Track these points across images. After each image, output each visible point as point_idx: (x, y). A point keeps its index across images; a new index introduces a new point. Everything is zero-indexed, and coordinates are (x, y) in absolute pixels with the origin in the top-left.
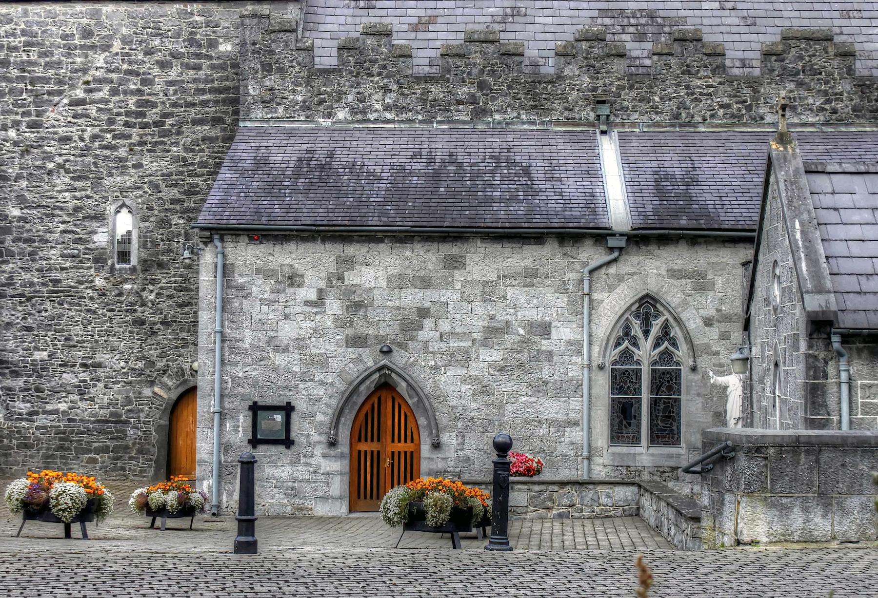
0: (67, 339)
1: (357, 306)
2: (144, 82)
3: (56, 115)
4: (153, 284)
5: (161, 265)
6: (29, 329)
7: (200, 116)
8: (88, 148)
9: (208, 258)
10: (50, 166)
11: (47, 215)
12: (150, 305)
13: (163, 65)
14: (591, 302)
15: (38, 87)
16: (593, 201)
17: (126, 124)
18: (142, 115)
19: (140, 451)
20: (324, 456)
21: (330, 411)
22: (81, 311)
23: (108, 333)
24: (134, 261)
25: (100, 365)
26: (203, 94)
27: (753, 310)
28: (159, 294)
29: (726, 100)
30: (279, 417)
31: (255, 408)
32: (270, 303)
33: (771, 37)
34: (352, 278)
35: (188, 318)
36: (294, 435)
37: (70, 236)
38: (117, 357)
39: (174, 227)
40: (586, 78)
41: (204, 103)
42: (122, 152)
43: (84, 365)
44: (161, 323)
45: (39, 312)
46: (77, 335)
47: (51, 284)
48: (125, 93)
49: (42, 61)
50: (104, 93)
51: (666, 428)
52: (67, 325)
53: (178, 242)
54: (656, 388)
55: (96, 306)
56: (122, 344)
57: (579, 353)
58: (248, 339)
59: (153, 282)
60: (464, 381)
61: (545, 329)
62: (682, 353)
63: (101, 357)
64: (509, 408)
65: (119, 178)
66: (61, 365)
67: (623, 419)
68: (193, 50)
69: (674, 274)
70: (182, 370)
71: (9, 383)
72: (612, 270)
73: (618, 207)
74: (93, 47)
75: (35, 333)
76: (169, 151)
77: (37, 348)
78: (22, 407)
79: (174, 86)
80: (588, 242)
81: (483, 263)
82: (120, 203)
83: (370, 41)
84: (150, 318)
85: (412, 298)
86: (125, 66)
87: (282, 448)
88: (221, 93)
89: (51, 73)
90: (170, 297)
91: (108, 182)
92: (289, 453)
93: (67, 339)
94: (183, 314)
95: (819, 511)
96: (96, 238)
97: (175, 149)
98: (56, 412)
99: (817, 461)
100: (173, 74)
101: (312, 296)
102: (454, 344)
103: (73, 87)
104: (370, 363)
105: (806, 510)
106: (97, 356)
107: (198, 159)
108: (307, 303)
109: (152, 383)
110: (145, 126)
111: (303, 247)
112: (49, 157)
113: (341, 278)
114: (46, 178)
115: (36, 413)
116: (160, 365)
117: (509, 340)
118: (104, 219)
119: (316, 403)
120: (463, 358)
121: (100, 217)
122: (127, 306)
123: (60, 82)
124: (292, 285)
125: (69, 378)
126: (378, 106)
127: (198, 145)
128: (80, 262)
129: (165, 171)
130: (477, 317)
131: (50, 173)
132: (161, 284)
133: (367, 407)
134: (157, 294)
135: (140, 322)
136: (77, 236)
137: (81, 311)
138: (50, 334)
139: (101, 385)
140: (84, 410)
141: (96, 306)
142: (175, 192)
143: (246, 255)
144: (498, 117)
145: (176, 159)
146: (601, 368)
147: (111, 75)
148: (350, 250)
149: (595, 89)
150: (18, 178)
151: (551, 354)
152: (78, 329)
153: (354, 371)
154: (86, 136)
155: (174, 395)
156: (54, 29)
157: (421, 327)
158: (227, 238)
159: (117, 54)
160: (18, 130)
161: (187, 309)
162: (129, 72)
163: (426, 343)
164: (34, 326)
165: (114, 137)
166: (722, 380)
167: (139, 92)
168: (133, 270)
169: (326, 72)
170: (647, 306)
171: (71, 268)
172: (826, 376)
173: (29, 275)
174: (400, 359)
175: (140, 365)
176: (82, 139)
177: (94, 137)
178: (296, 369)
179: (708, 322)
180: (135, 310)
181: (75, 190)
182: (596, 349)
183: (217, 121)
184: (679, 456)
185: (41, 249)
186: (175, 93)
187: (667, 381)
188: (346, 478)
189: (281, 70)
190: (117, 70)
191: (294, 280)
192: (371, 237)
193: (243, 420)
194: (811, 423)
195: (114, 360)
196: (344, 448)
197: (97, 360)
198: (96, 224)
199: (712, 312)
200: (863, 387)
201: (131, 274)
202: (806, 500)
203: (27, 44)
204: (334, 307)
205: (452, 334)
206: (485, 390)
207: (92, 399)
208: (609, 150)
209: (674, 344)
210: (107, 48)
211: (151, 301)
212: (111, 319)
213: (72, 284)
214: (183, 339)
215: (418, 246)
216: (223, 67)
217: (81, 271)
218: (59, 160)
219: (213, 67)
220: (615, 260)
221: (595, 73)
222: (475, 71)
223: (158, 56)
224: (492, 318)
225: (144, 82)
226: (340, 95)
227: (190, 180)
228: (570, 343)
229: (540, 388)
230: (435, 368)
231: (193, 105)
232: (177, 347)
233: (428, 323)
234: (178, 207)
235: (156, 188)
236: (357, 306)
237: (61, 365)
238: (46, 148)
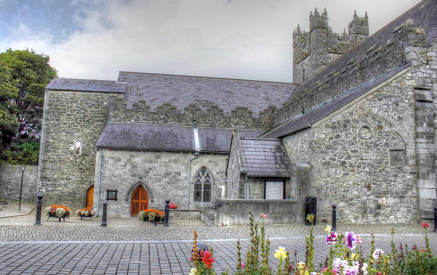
1: (134, 167)
2: (85, 111)
3: (63, 118)
5: (87, 155)
6: (53, 170)
8: (70, 126)
9: (98, 154)
10: (61, 130)
13: (90, 107)
14: (190, 168)
15: (59, 111)
16: (192, 143)
17: (80, 121)
18: (84, 119)
19: (79, 201)
20: (125, 203)
21: (127, 192)
23: (73, 171)
24: (80, 154)
25: (70, 179)
27: (228, 171)
29: (223, 122)
30: (114, 193)
31: (108, 191)
32: (113, 165)
33: (234, 108)
34: (133, 160)
36: (117, 198)
40: (191, 115)
41: (99, 117)
42: (79, 127)
43: (66, 179)
48: (80, 113)
49: (61, 104)
50: (75, 113)
51: (207, 198)
54: (205, 188)
57: (187, 180)
58: (107, 174)
59: (84, 159)
60: (159, 186)
61: (179, 174)
62: (211, 180)
63: (70, 177)
64: (170, 192)
67: (197, 195)
68: (98, 104)
69: (210, 162)
71: (47, 183)
72: (196, 160)
73: (197, 146)
74: (73, 102)
77: (55, 174)
78: (50, 189)
80: (190, 153)
81: (165, 158)
83: (140, 104)
85: (148, 165)
86: (81, 107)
87: (114, 201)
89: (62, 108)
90: (89, 163)
91: (75, 134)
92: (116, 202)
95: (241, 218)
96: (71, 148)
98: (59, 190)
99: (241, 206)
100: (92, 109)
101: (124, 164)
102: (157, 177)
103: (68, 111)
104: (137, 181)
105: (238, 218)
108: (122, 166)
109: (83, 184)
110: (85, 121)
111: (122, 152)
112: (61, 128)
113: (131, 160)
115: (54, 190)
116: (85, 179)
117: (171, 176)
119: (123, 191)
120: (159, 180)
121: (72, 143)
123: (65, 110)
124: (118, 161)
125: (62, 182)
126: (142, 119)
130: (163, 170)
131: (61, 132)
133: (136, 191)
135: (81, 169)
139: (70, 184)
140: (66, 190)
143: (107, 154)
144: (170, 123)
145: (92, 130)
146: (192, 183)
148: (133, 153)
149: (193, 118)
150: (53, 132)
151: (180, 180)
153: (133, 182)
155: (88, 187)
156: (64, 97)
157: (149, 172)
158: (103, 149)
162: (81, 108)
163: (150, 176)
166: (220, 187)
167: (84, 113)
168: (80, 156)
169: (129, 110)
170: (203, 169)
172: (244, 187)
174: (144, 180)
175: (80, 179)
176: (69, 124)
177: (72, 123)
178: (119, 182)
179: (218, 173)
181: (66, 136)
182: (191, 179)
183: (102, 121)
184: (210, 205)
187: (208, 187)
188: (130, 209)
189: (118, 110)
190: (79, 108)
191: (119, 160)
192: (138, 150)
193: (105, 193)
194: (240, 197)
196: (130, 201)
199: (219, 171)
200: (252, 189)
202: (239, 215)
203: (57, 101)
204: (128, 167)
205: (157, 174)
206: (164, 188)
207: (68, 187)
208: (196, 132)
209: (210, 178)
210: (77, 102)
215: (149, 153)
216: (105, 108)
218: (63, 129)
219: (102, 108)
220: (196, 158)
221: (193, 114)
222: (165, 112)
223: (89, 105)
224: (167, 171)
225: (85, 111)
226: (133, 116)
227: (95, 135)
228: (185, 177)
229: (178, 188)
230: (153, 182)
231: (97, 117)
233: (151, 171)
235: (87, 136)
236: (134, 167)
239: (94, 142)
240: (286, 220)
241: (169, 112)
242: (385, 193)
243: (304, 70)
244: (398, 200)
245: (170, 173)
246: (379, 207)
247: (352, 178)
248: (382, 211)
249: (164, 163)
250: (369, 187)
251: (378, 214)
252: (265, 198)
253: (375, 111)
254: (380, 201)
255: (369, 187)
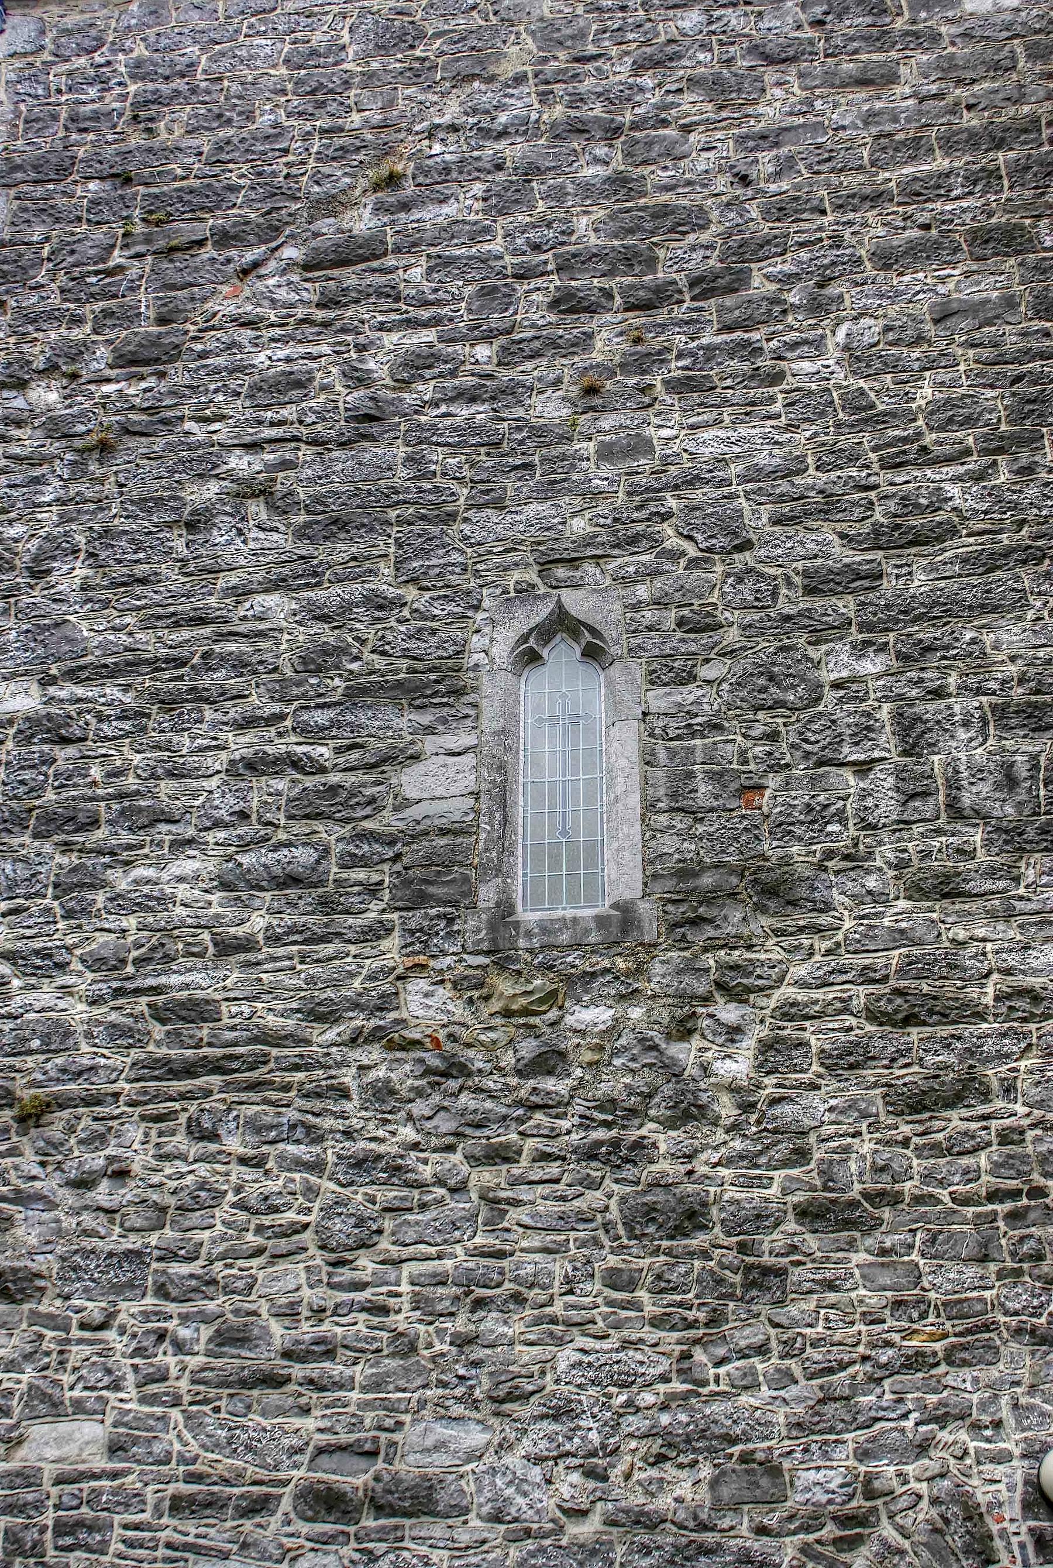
0: (231, 1338)
4: (737, 995)
5: (775, 891)
7: (914, 233)
11: (168, 703)
12: (726, 1108)
22: (316, 1167)
26: (913, 158)
28: (774, 1052)
35: (971, 1175)
37: (280, 785)
38: (538, 1437)
39: (830, 696)
43: (324, 1502)
44: (803, 1213)
45: (83, 1183)
46: (290, 1313)
47: (158, 1031)
52: (229, 1256)
53: (863, 768)
55: (408, 1133)
56: (566, 1356)
65: (533, 509)
66: (178, 1505)
70: (972, 1514)
75: (48, 1306)
76: (776, 378)
77: (48, 1405)
79: (777, 145)
82: (543, 611)
84: (727, 1188)
88: (999, 145)
90: (846, 1061)
93: (231, 1338)
94: (936, 1150)
96: (411, 781)
97: (807, 366)
106: (411, 1435)
107: (926, 393)
114: (179, 546)
118: (458, 692)
121: (439, 687)
122: (586, 1123)
127: (919, 340)
128: (326, 905)
129: (762, 459)
131: (196, 523)
132: (788, 991)
134: (766, 1047)
136: (309, 782)
137: (316, 1167)
138: (128, 1309)
141: (408, 1133)
142: (826, 543)
145: (810, 405)
147: (490, 149)
152: (292, 1279)
154: (377, 366)
159: (519, 79)
160: (74, 376)
161: (955, 1120)
164: (40, 1263)
165: (506, 358)
171: (274, 939)
173: (45, 996)
175: (685, 1488)
180: (638, 1145)
181: (314, 577)
185: (119, 857)
186: (785, 167)
195: (513, 1460)
197: (408, 1467)
198: (406, 721)
201: (610, 945)
211: (733, 1089)
212: (495, 1205)
213: (272, 1020)
214: (954, 1308)
217: (329, 949)
232: (916, 1361)
234: (847, 606)
237: (178, 1505)
238: (189, 425)
239: (911, 612)
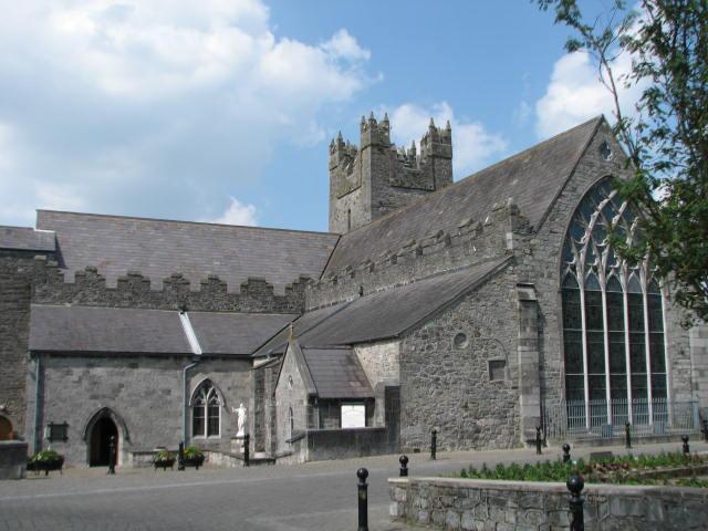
1: (95, 383)
16: (186, 343)
27: (277, 390)
33: (245, 280)
54: (209, 414)
61: (168, 392)
62: (219, 399)
73: (196, 349)
101: (77, 379)
108: (74, 382)
117: (155, 396)
119: (78, 424)
148: (93, 361)
151: (170, 402)
170: (206, 384)
174: (111, 404)
179: (229, 389)
187: (213, 411)
194: (310, 427)
196: (88, 441)
199: (230, 385)
204: (85, 383)
208: (185, 319)
219: (15, 279)
229: (168, 415)
236: (95, 383)
240: (374, 451)
241: (135, 289)
242: (485, 414)
243: (349, 211)
244: (497, 421)
245: (154, 392)
246: (478, 431)
247: (446, 398)
248: (481, 435)
249: (142, 377)
250: (466, 407)
251: (477, 439)
252: (340, 426)
253: (472, 314)
254: (478, 422)
255: (466, 407)
